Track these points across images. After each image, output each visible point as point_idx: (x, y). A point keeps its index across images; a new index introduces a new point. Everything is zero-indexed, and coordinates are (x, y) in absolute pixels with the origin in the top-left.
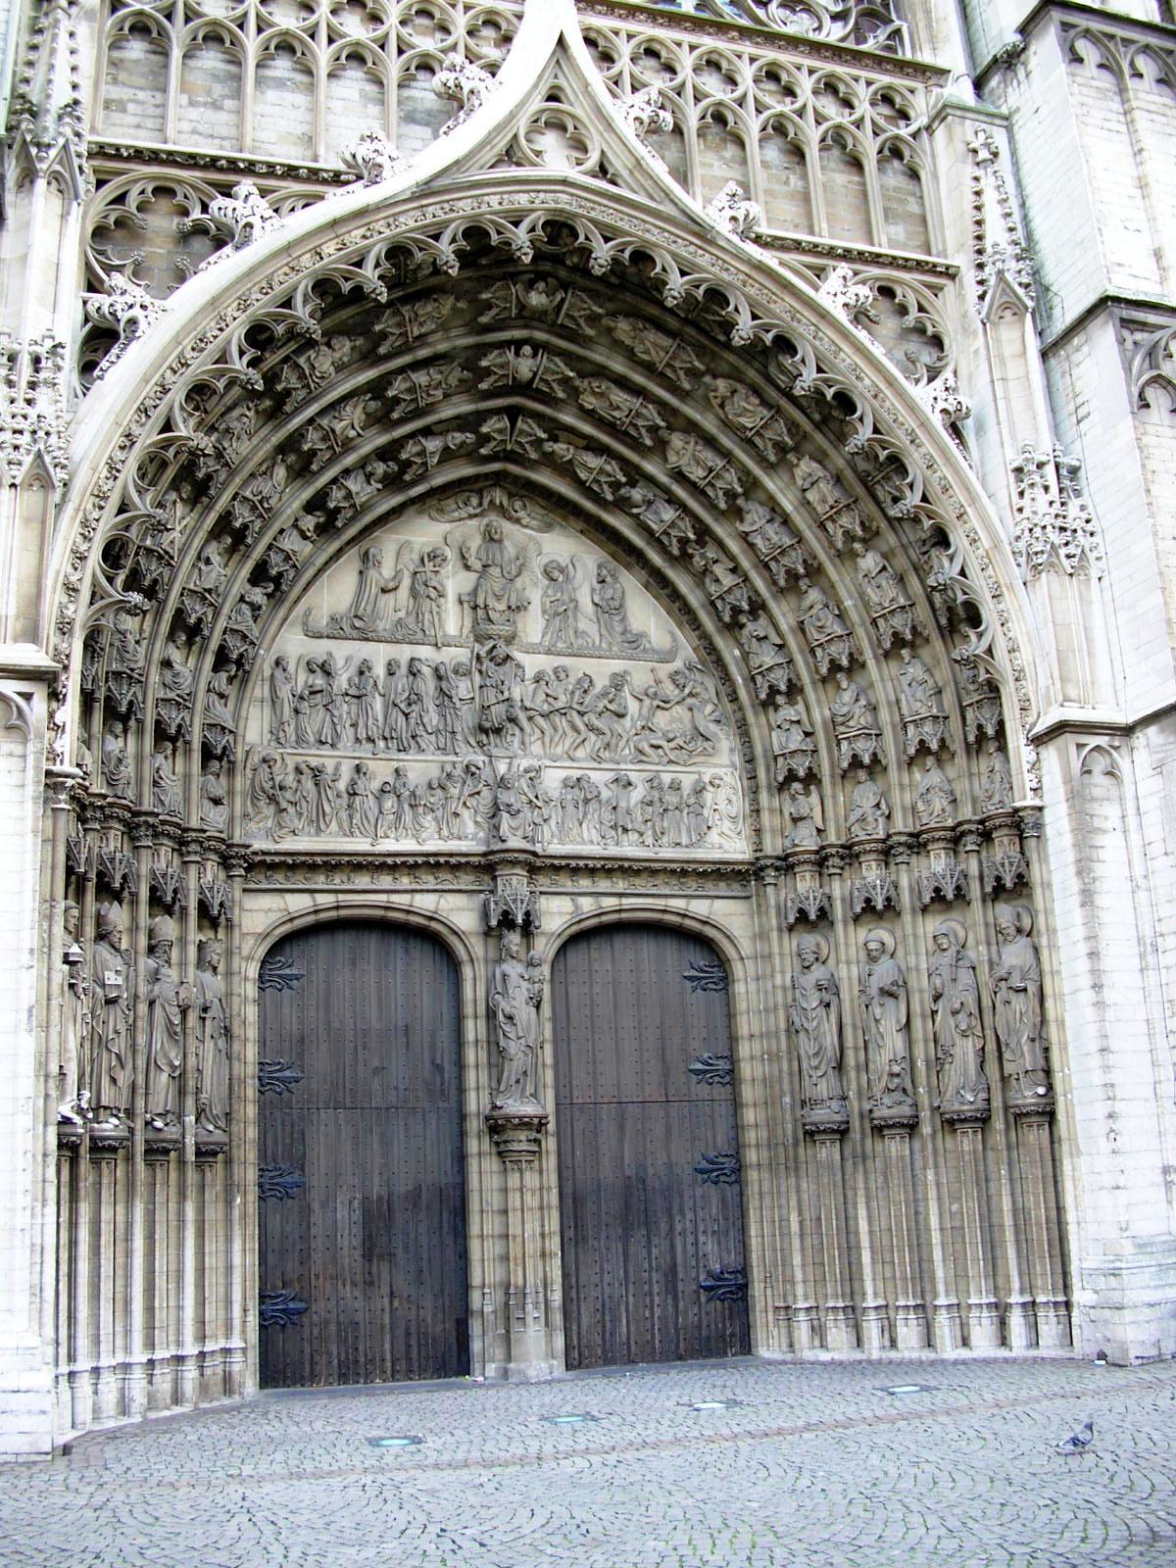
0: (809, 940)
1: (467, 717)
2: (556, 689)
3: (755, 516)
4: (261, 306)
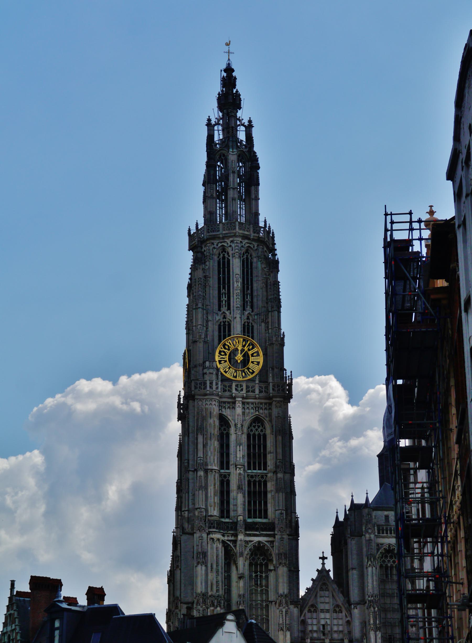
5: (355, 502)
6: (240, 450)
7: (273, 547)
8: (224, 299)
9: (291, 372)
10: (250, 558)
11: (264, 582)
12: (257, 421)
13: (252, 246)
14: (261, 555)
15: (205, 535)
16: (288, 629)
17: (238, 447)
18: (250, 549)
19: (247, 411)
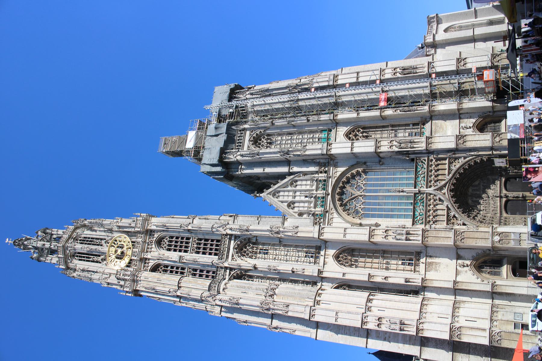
4: (460, 213)
6: (171, 258)
10: (246, 257)
12: (159, 243)
14: (246, 248)
19: (153, 250)
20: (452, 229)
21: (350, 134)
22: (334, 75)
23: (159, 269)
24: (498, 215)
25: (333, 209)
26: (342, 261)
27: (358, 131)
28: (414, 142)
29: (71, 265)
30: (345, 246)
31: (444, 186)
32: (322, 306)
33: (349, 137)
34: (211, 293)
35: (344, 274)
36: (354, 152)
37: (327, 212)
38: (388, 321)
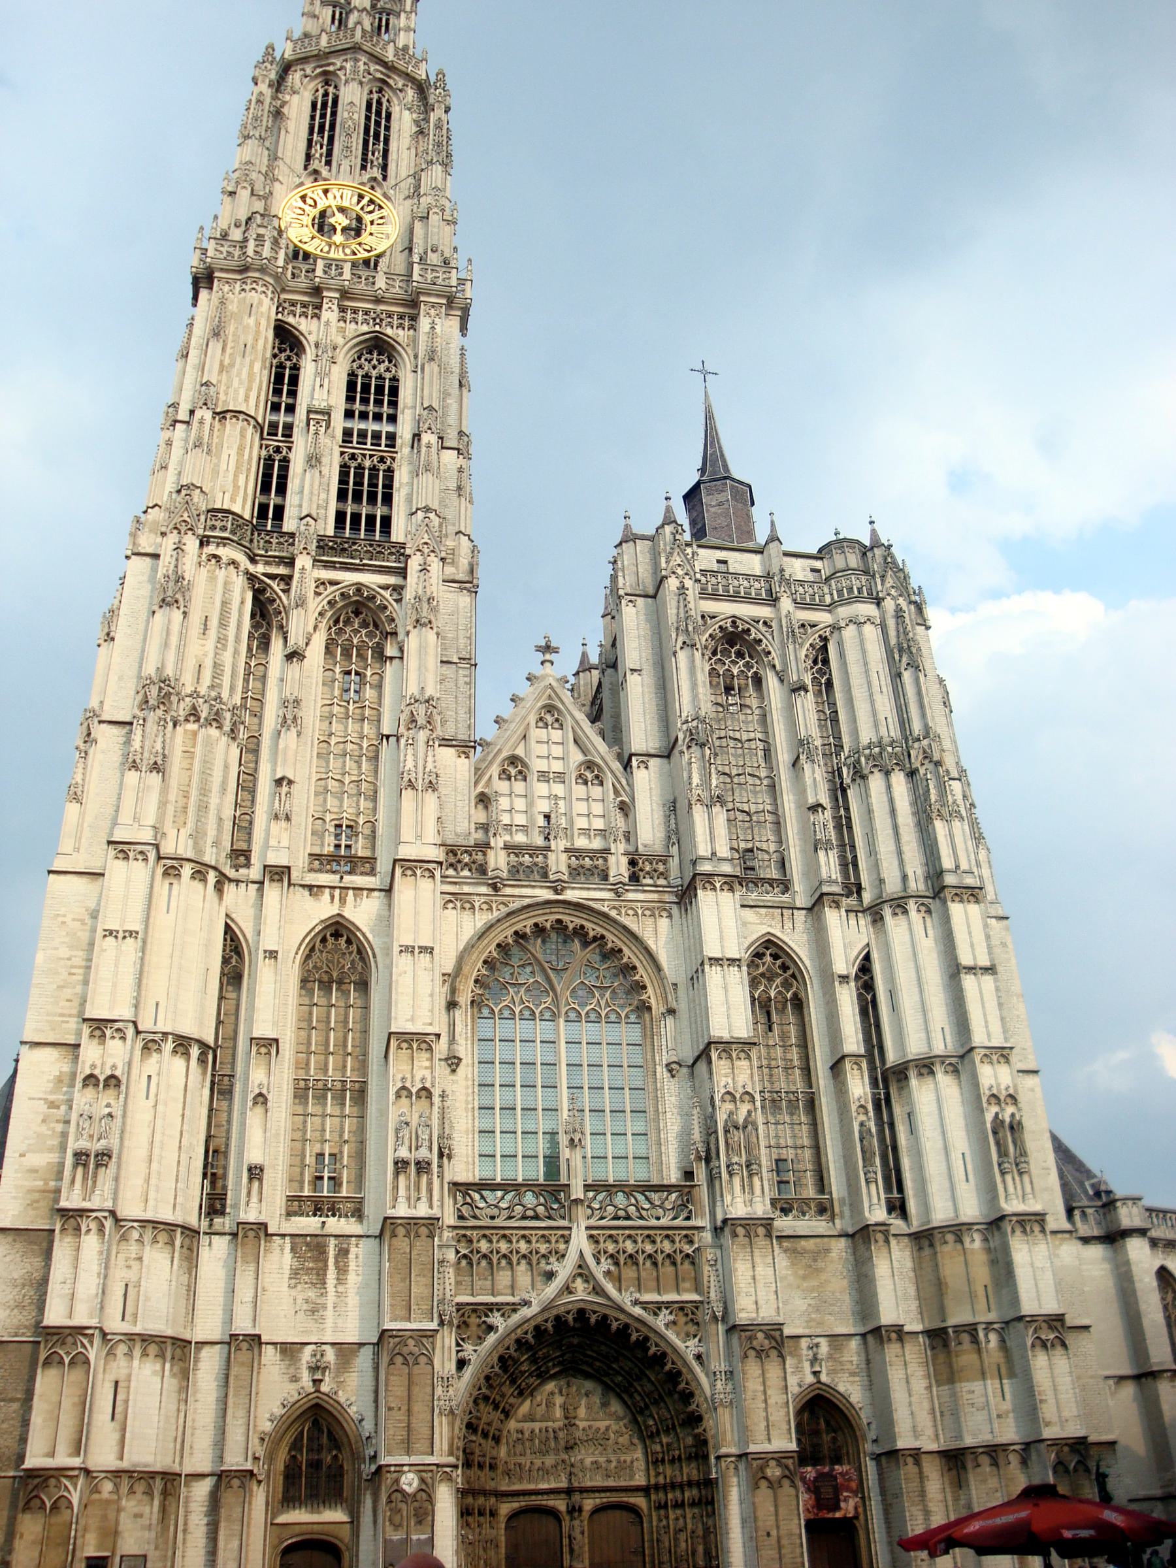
0: (662, 1512)
1: (562, 1443)
2: (589, 1432)
3: (645, 1380)
4: (501, 1350)
5: (637, 529)
6: (321, 385)
7: (399, 601)
8: (317, 151)
9: (470, 260)
10: (330, 628)
11: (369, 693)
12: (378, 346)
13: (391, 82)
14: (364, 624)
15: (192, 544)
16: (432, 786)
17: (318, 379)
18: (329, 602)
20: (442, 1323)
21: (775, 957)
22: (981, 889)
23: (285, 350)
24: (504, 1488)
25: (504, 910)
26: (325, 947)
27: (786, 985)
28: (751, 1176)
29: (295, 77)
30: (374, 957)
31: (598, 1289)
32: (161, 886)
33: (764, 954)
34: (203, 518)
35: (272, 954)
36: (707, 967)
37: (494, 887)
38: (107, 1111)
